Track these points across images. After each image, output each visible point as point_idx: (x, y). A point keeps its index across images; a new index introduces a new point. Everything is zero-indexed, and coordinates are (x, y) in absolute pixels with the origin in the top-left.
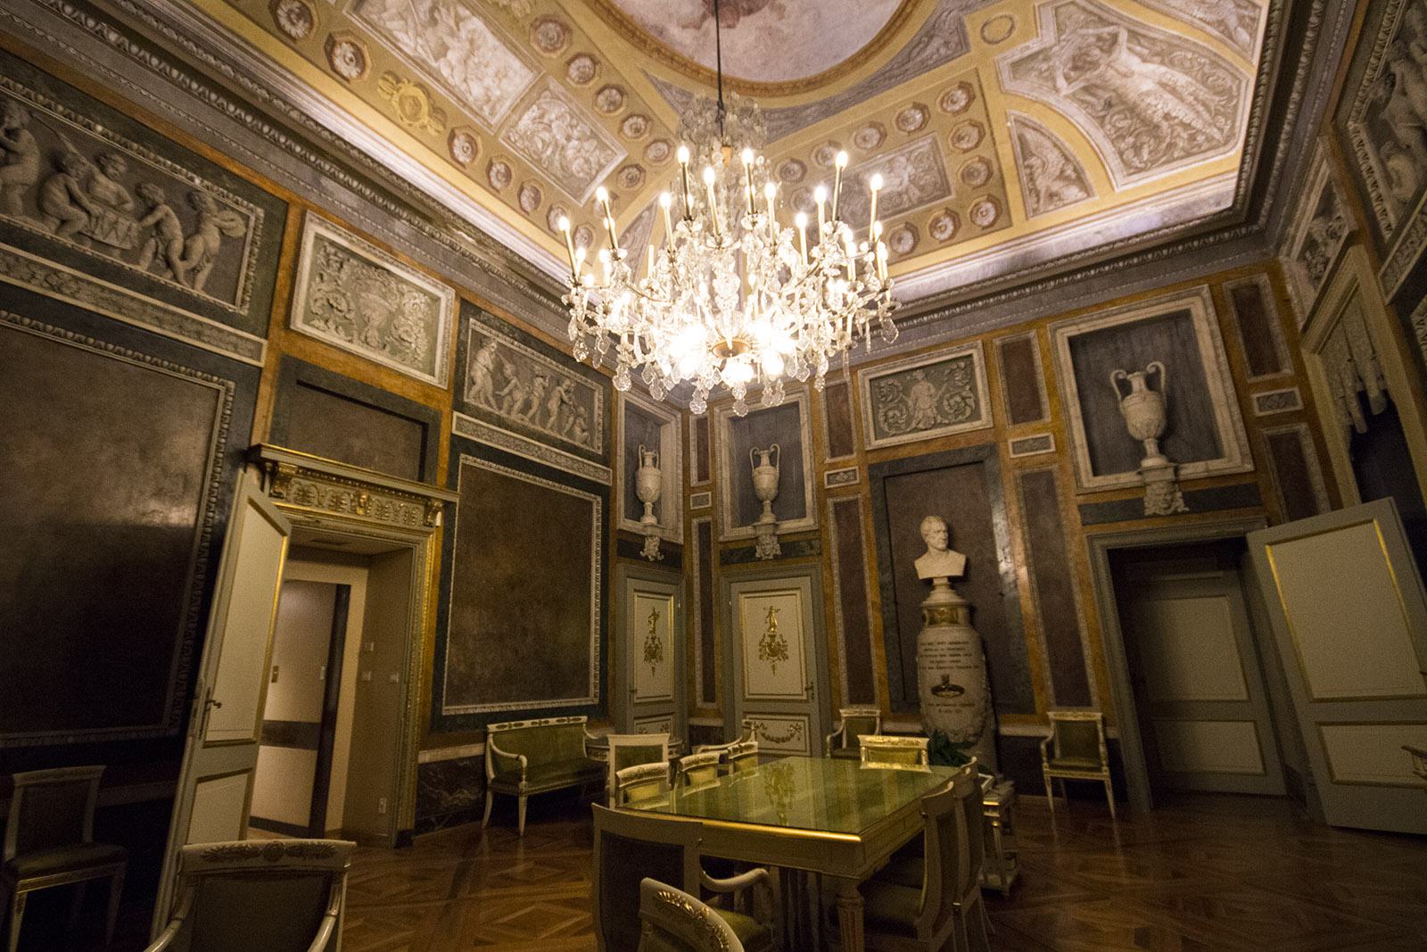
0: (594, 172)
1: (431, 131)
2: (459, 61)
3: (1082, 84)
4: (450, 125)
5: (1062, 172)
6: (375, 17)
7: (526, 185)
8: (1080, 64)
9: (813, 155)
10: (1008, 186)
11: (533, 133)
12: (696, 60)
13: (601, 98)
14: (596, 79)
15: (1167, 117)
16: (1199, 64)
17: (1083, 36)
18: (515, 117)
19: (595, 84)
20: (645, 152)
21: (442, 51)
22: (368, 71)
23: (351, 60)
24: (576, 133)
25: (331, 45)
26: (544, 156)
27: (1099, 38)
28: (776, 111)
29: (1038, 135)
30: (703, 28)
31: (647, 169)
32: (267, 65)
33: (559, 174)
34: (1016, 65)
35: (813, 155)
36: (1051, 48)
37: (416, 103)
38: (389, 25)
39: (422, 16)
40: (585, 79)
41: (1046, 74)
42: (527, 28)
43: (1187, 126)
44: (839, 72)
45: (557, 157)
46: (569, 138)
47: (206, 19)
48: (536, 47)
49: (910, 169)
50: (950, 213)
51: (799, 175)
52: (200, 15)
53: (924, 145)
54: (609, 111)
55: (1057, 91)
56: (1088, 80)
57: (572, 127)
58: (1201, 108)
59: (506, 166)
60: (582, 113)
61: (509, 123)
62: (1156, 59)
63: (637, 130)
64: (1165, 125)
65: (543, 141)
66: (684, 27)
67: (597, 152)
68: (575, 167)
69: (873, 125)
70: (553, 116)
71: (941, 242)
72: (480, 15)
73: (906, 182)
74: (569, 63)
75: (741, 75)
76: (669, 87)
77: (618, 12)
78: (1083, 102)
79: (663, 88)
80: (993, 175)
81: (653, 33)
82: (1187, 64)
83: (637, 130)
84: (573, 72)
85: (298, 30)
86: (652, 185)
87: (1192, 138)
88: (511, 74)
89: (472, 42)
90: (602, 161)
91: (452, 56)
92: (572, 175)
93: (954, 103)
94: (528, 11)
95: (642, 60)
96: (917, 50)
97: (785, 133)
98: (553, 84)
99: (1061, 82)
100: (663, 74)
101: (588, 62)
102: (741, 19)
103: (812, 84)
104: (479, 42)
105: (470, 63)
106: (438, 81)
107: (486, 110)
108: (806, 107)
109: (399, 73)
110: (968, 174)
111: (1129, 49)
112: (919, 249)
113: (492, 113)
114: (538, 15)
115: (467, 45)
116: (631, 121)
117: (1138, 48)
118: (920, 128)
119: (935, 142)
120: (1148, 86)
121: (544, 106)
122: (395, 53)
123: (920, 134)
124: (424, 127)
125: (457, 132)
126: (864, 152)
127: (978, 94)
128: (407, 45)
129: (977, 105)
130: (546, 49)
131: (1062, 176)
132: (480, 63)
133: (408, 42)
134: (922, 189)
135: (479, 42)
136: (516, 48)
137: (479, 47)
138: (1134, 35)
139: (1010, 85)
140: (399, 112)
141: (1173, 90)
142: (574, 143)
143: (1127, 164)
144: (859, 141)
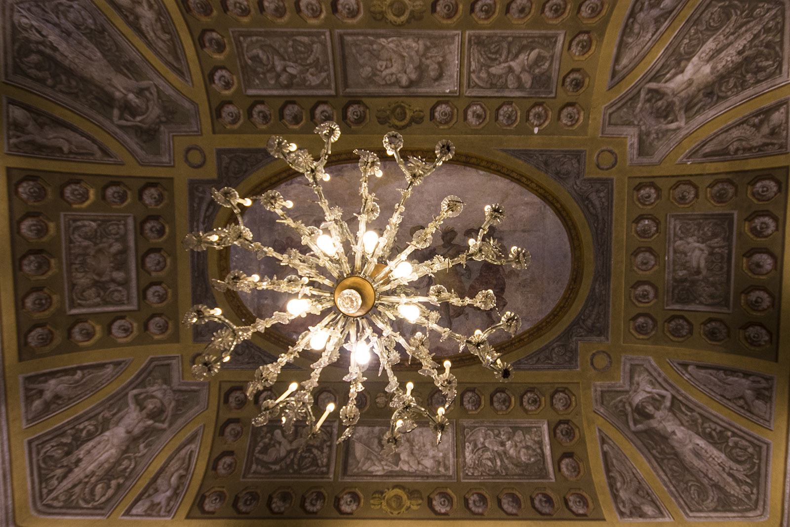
0: (539, 451)
1: (415, 508)
2: (409, 456)
3: (682, 112)
4: (425, 495)
5: (754, 126)
6: (355, 470)
7: (502, 496)
8: (664, 114)
9: (637, 303)
10: (747, 168)
14: (483, 398)
15: (740, 53)
16: (696, 33)
17: (641, 110)
18: (461, 460)
20: (555, 409)
21: (397, 458)
22: (362, 501)
23: (351, 501)
25: (338, 500)
26: (498, 468)
27: (649, 100)
29: (711, 143)
31: (569, 417)
33: (518, 471)
34: (642, 152)
35: (637, 303)
36: (641, 131)
37: (398, 498)
39: (377, 450)
40: (477, 404)
41: (660, 135)
43: (756, 36)
45: (506, 461)
46: (503, 444)
49: (690, 240)
50: (750, 219)
51: (650, 322)
53: (674, 225)
54: (508, 407)
55: (679, 128)
56: (680, 109)
58: (744, 29)
59: (478, 494)
60: (495, 422)
61: (460, 464)
62: (683, 64)
64: (746, 53)
65: (489, 459)
67: (528, 436)
69: (635, 254)
70: (482, 440)
71: (777, 229)
73: (702, 246)
78: (698, 112)
80: (730, 179)
82: (695, 42)
83: (535, 401)
86: (585, 425)
87: (767, 30)
89: (408, 440)
91: (404, 456)
93: (649, 196)
99: (673, 126)
105: (415, 452)
106: (404, 476)
107: (442, 469)
108: (593, 290)
110: (720, 198)
111: (666, 82)
112: (777, 251)
113: (447, 468)
115: (407, 444)
117: (668, 76)
118: (658, 224)
119: (676, 217)
120: (707, 69)
121: (472, 438)
122: (374, 480)
123: (662, 226)
124: (408, 508)
125: (432, 496)
126: (656, 268)
127: (652, 180)
128: (378, 471)
129: (659, 182)
131: (757, 127)
132: (420, 447)
133: (378, 469)
134: (715, 235)
137: (414, 440)
138: (655, 78)
139: (656, 158)
140: (389, 510)
141: (719, 51)
142: (508, 444)
143: (771, 76)
144: (644, 267)
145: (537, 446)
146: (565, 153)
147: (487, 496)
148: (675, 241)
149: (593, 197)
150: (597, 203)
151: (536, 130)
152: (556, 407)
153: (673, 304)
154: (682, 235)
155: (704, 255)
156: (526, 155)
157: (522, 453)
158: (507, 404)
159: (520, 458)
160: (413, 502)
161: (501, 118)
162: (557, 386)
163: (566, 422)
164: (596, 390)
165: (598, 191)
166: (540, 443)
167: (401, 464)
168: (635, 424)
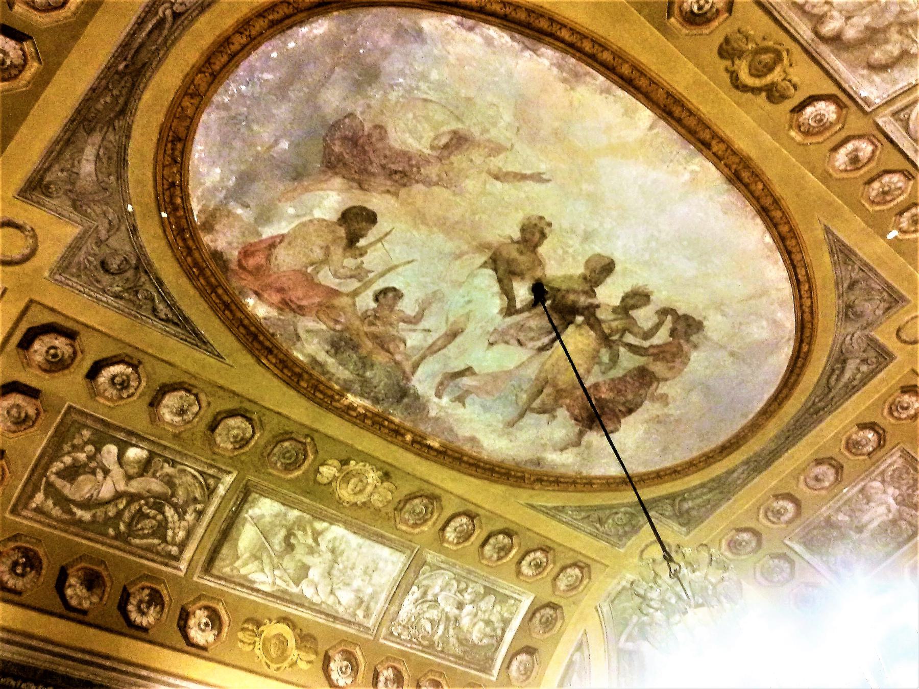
0: (499, 632)
1: (302, 665)
2: (323, 576)
4: (322, 648)
6: (227, 570)
9: (761, 516)
11: (418, 617)
12: (585, 473)
13: (488, 548)
18: (394, 609)
19: (479, 535)
22: (225, 629)
23: (207, 625)
24: (468, 597)
25: (184, 617)
26: (436, 638)
28: (695, 488)
30: (583, 443)
31: (562, 602)
32: (121, 672)
33: (458, 651)
37: (282, 640)
38: (243, 571)
39: (277, 547)
40: (465, 536)
42: (391, 515)
44: (754, 426)
45: (451, 632)
46: (460, 606)
47: (57, 649)
48: (404, 528)
49: (891, 490)
52: (50, 647)
54: (499, 558)
57: (461, 592)
59: (394, 668)
60: (469, 572)
61: (389, 616)
63: (538, 566)
65: (432, 621)
66: (562, 450)
67: (498, 608)
68: (475, 636)
70: (437, 589)
72: (338, 521)
74: (443, 529)
75: (642, 470)
76: (561, 509)
77: (486, 463)
79: (554, 513)
81: (530, 468)
83: (538, 566)
84: (450, 534)
85: (149, 619)
86: (573, 620)
88: (381, 565)
89: (333, 551)
90: (506, 615)
91: (315, 574)
92: (474, 645)
94: (390, 497)
95: (524, 495)
96: (834, 377)
97: (716, 506)
98: (431, 556)
100: (550, 499)
101: (464, 520)
102: (622, 421)
103: (726, 449)
104: (342, 547)
105: (335, 572)
106: (302, 605)
107: (360, 613)
108: (731, 472)
109: (258, 616)
113: (367, 615)
114: (402, 496)
115: (329, 556)
116: (528, 559)
118: (880, 445)
121: (425, 582)
122: (253, 597)
123: (881, 452)
125: (331, 653)
126: (824, 492)
128: (263, 583)
130: (415, 525)
133: (264, 580)
135: (342, 547)
136: (382, 536)
137: (342, 553)
142: (468, 608)
144: (812, 483)
145: (501, 625)
146: (889, 288)
147: (406, 676)
148: (875, 480)
149: (851, 365)
150: (848, 375)
151: (893, 234)
152: (558, 583)
153: (798, 542)
154: (888, 479)
155: (885, 518)
156: (843, 253)
157: (477, 627)
158: (502, 554)
159: (471, 634)
160: (302, 654)
161: (876, 185)
162: (580, 558)
163: (554, 607)
164: (619, 583)
165: (864, 361)
166: (506, 622)
167: (304, 584)
168: (627, 640)
